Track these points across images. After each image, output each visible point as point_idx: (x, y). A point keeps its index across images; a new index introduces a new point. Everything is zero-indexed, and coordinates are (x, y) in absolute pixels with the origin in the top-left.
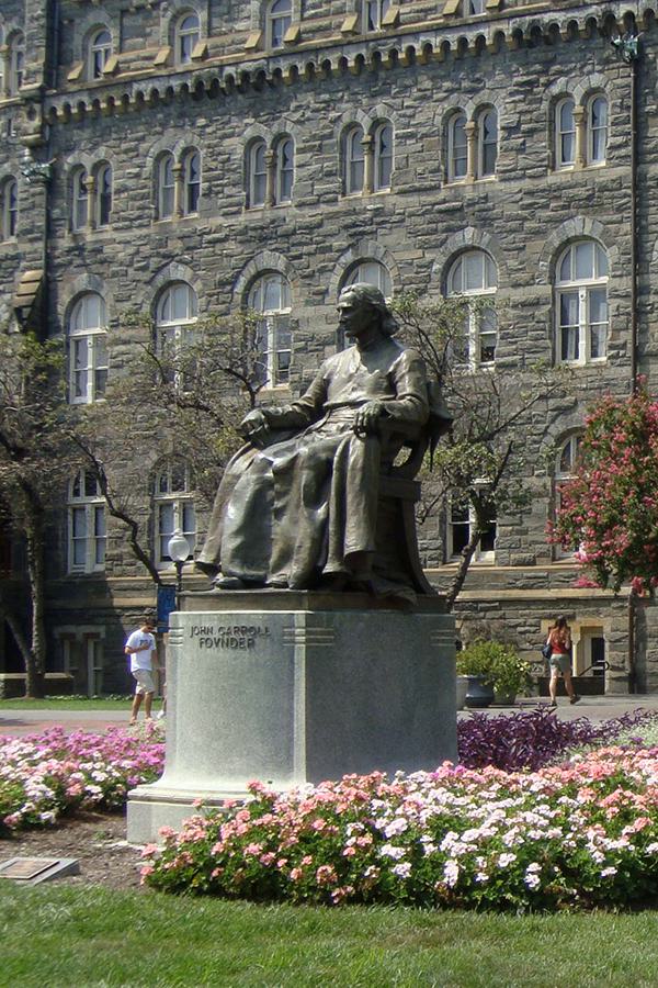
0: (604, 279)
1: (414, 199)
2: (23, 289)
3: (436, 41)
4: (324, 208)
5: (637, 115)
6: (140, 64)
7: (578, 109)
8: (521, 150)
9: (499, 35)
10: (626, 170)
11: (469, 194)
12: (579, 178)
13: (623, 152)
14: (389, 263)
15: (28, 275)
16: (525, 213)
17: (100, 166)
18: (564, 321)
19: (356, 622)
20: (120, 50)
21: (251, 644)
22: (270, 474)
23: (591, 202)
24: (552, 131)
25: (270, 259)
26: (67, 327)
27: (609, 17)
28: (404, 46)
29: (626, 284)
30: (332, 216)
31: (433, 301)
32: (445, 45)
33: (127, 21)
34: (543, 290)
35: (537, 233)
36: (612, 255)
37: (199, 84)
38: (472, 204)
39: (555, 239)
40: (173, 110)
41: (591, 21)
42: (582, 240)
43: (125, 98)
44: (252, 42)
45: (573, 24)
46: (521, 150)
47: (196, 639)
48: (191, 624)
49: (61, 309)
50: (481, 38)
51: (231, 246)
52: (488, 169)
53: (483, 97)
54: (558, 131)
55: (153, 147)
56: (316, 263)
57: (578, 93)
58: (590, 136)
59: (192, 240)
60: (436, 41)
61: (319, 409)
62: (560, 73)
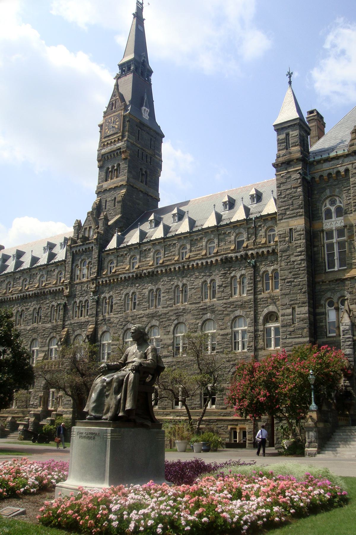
0: (246, 328)
1: (193, 306)
2: (89, 330)
3: (200, 262)
4: (169, 308)
5: (254, 282)
6: (121, 270)
7: (238, 280)
8: (223, 292)
9: (217, 260)
10: (252, 297)
11: (209, 304)
12: (239, 299)
13: (251, 292)
14: (187, 323)
15: (91, 326)
16: (224, 309)
17: (111, 297)
18: (235, 339)
19: (129, 432)
20: (117, 266)
21: (94, 438)
22: (105, 384)
24: (231, 286)
25: (155, 322)
26: (101, 341)
27: (246, 255)
28: (191, 264)
29: (252, 329)
30: (172, 310)
31: (199, 333)
32: (202, 263)
33: (118, 259)
34: (229, 331)
35: (228, 315)
36: (248, 320)
37: (137, 275)
38: (209, 307)
39: (232, 316)
40: (130, 282)
41: (241, 256)
42: (240, 316)
43: (118, 279)
44: (151, 264)
45: (237, 257)
46: (223, 292)
49: (99, 336)
50: (212, 261)
51: (144, 319)
52: (214, 297)
53: (213, 277)
54: (233, 286)
55: (124, 292)
56: (167, 323)
57: (238, 276)
58: (242, 288)
59: (134, 318)
60: (200, 262)
61: (125, 364)
62: (233, 270)
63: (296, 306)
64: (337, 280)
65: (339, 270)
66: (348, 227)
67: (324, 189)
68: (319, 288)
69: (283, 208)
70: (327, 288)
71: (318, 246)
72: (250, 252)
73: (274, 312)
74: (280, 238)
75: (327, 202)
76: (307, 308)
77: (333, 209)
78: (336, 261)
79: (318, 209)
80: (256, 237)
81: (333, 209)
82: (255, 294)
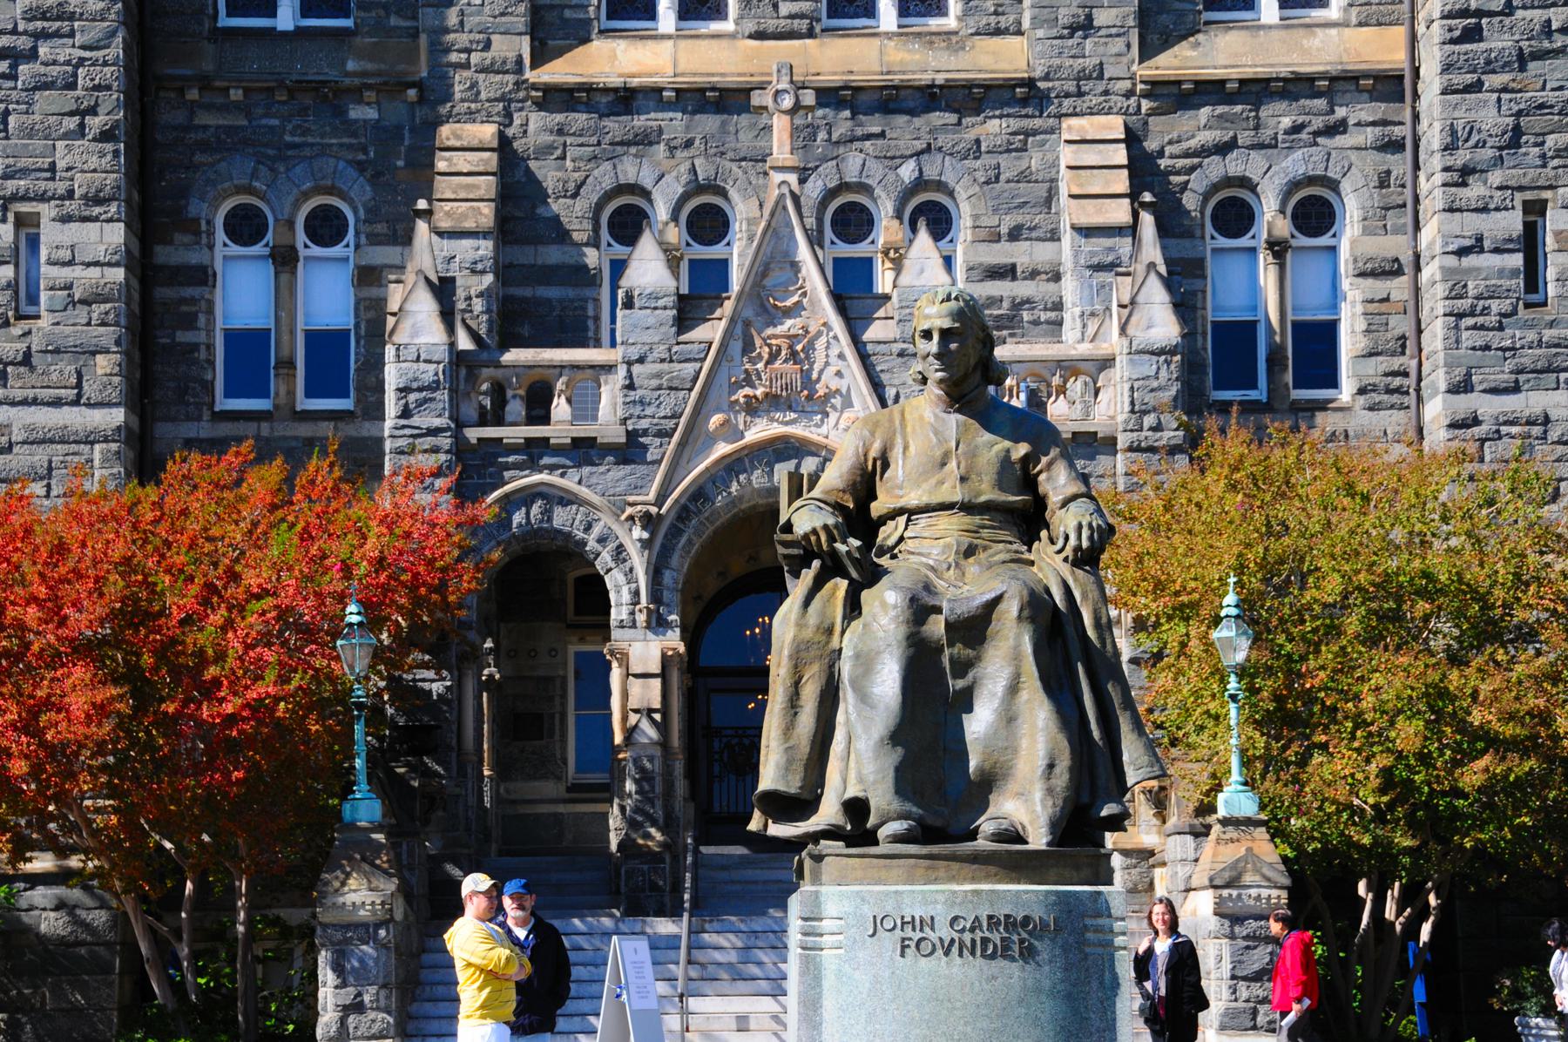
47: (889, 942)
63: (47, 211)
65: (300, 32)
68: (179, 117)
70: (230, 130)
76: (116, 234)
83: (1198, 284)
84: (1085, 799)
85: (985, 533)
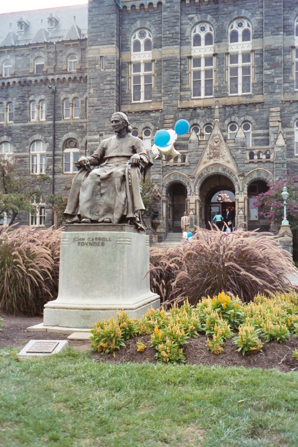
5: (54, 107)
9: (14, 82)
16: (22, 133)
18: (33, 162)
21: (103, 244)
23: (41, 129)
27: (47, 80)
41: (41, 80)
47: (76, 243)
48: (73, 237)
50: (9, 83)
53: (10, 100)
57: (37, 100)
58: (40, 112)
62: (32, 94)
63: (103, 132)
64: (142, 112)
66: (156, 62)
67: (135, 20)
69: (94, 34)
71: (125, 77)
72: (50, 77)
73: (74, 139)
74: (90, 65)
75: (137, 33)
77: (142, 42)
78: (142, 93)
79: (127, 40)
80: (56, 62)
81: (142, 42)
82: (54, 119)
83: (293, 136)
84: (125, 214)
85: (122, 162)
